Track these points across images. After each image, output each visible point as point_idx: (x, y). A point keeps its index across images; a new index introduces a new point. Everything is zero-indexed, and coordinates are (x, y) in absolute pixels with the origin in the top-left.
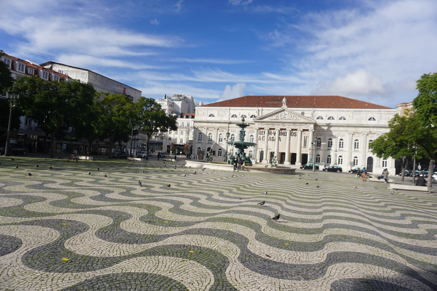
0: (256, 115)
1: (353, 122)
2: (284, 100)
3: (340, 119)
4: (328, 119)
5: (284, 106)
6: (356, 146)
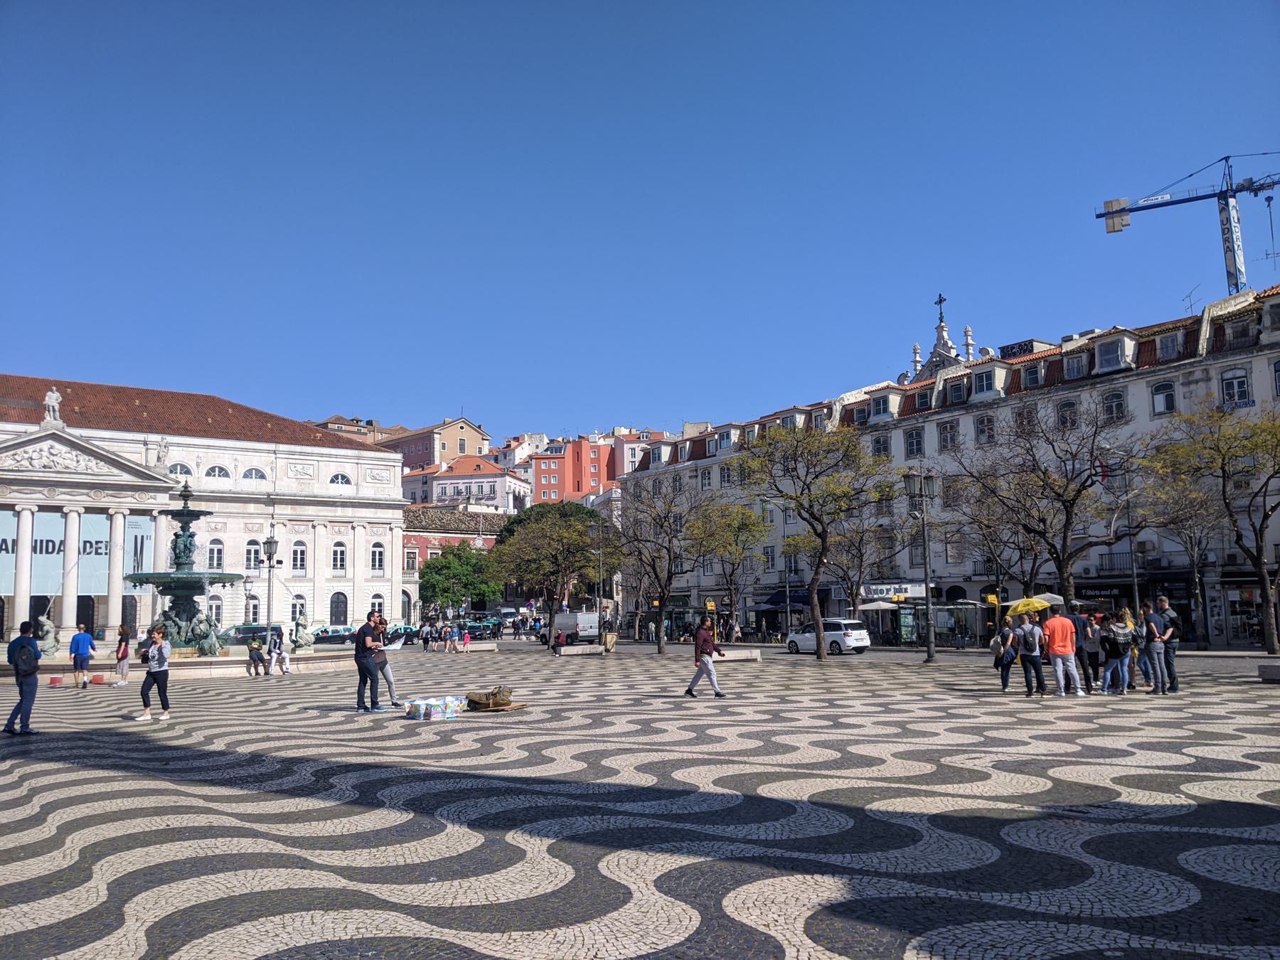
1: (287, 486)
2: (53, 399)
3: (247, 475)
4: (208, 474)
5: (52, 422)
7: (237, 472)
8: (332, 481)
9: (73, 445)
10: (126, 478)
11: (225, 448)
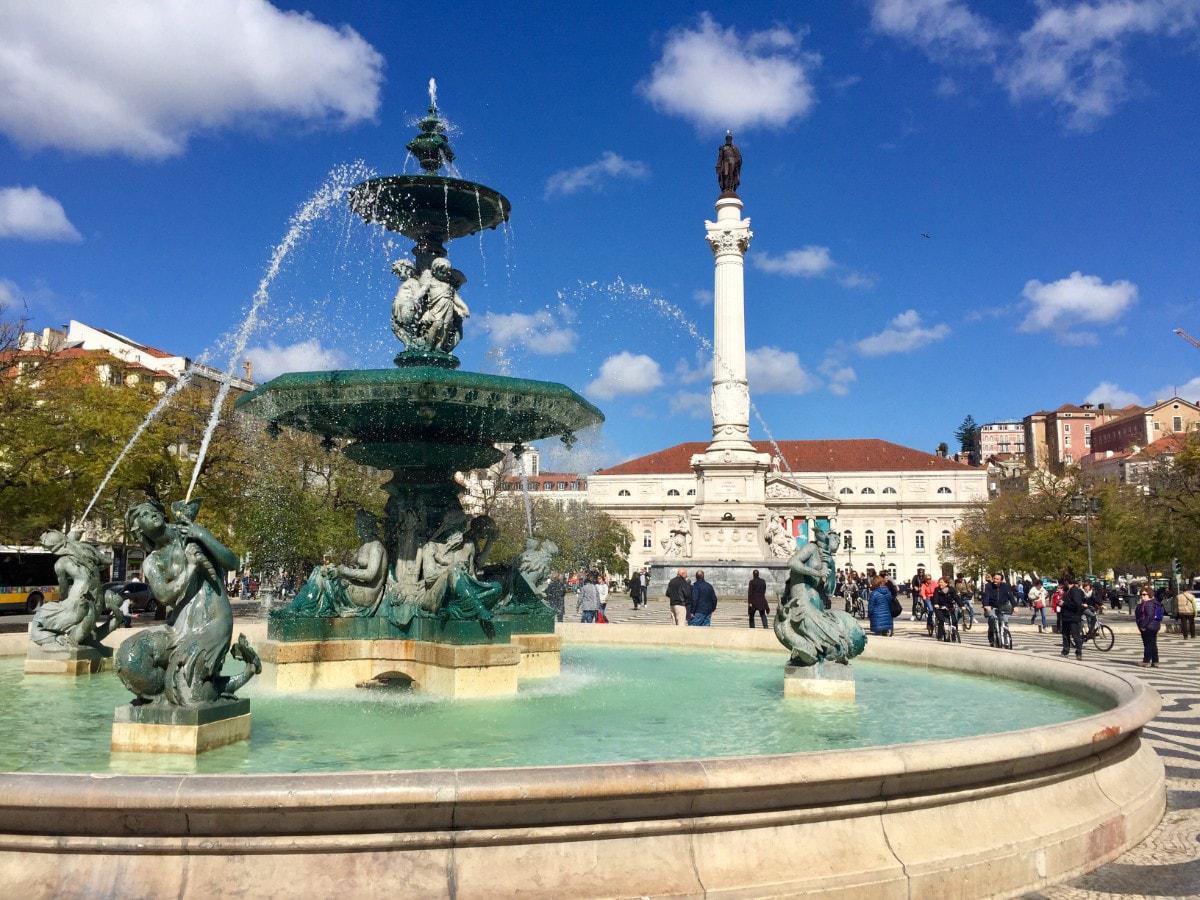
3: (884, 492)
6: (920, 542)
7: (878, 491)
8: (939, 492)
9: (787, 485)
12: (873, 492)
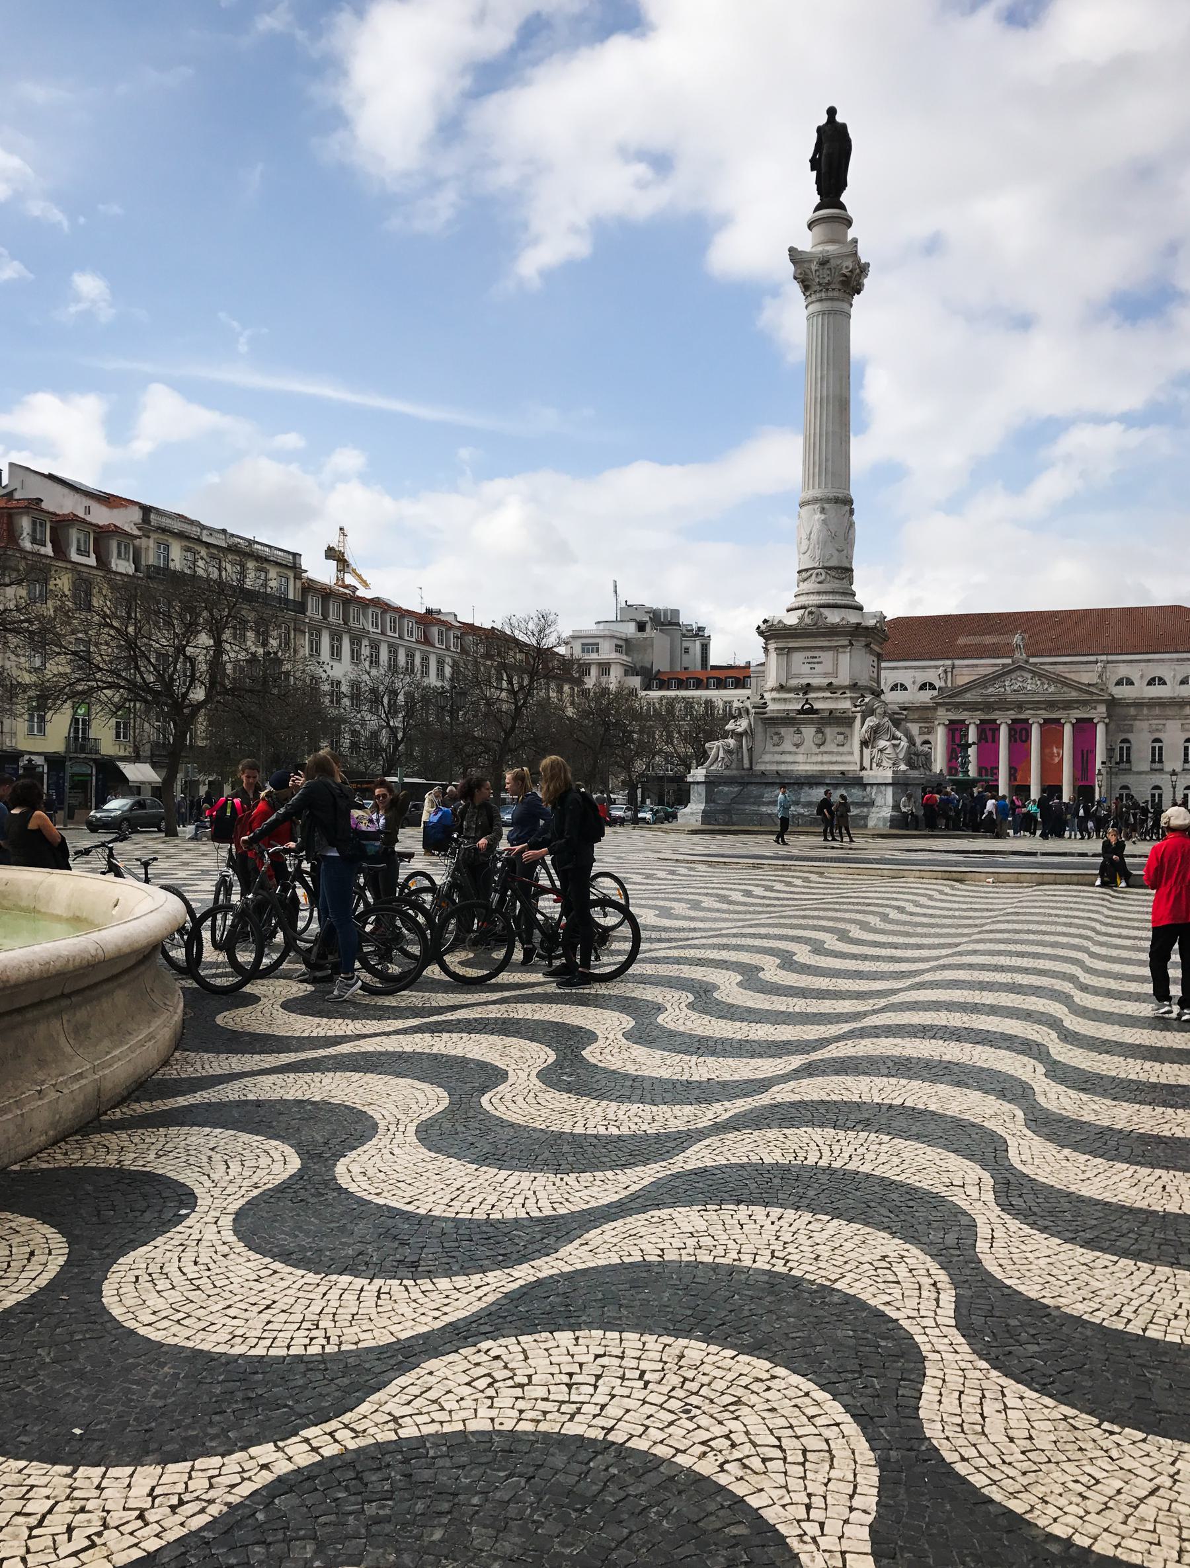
0: (938, 684)
4: (1149, 684)
10: (1074, 695)
11: (1163, 660)
12: (1165, 683)
